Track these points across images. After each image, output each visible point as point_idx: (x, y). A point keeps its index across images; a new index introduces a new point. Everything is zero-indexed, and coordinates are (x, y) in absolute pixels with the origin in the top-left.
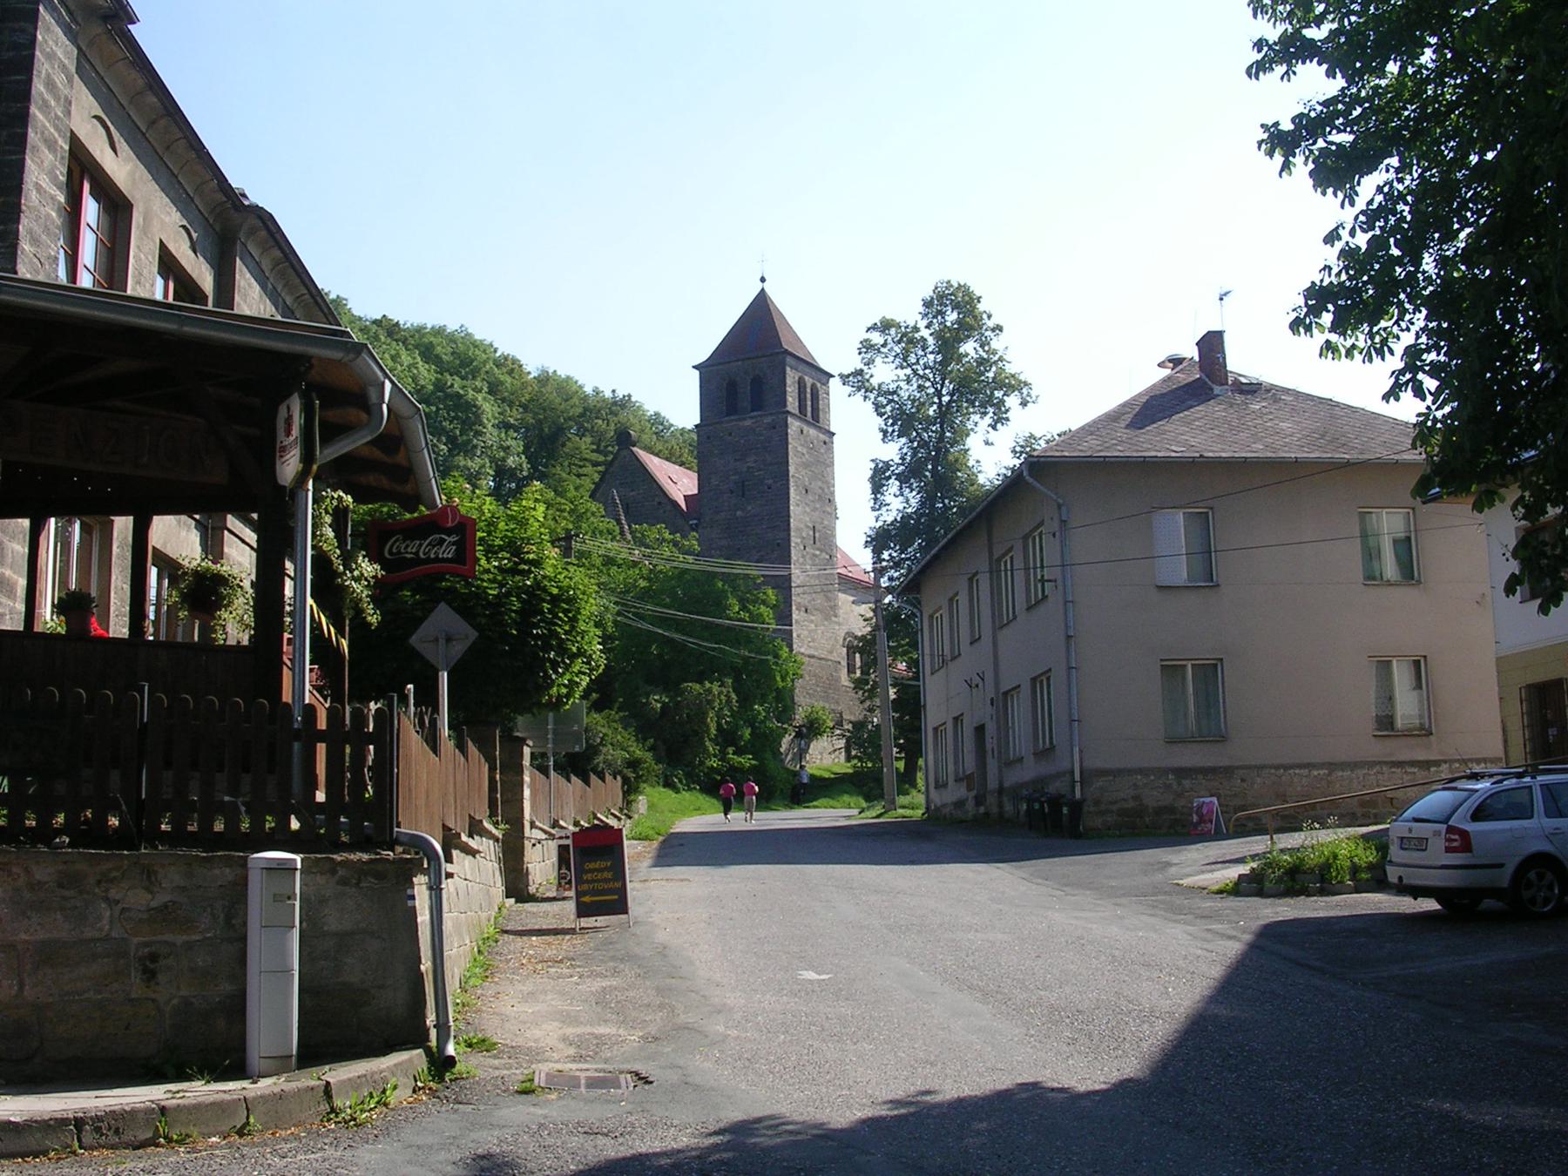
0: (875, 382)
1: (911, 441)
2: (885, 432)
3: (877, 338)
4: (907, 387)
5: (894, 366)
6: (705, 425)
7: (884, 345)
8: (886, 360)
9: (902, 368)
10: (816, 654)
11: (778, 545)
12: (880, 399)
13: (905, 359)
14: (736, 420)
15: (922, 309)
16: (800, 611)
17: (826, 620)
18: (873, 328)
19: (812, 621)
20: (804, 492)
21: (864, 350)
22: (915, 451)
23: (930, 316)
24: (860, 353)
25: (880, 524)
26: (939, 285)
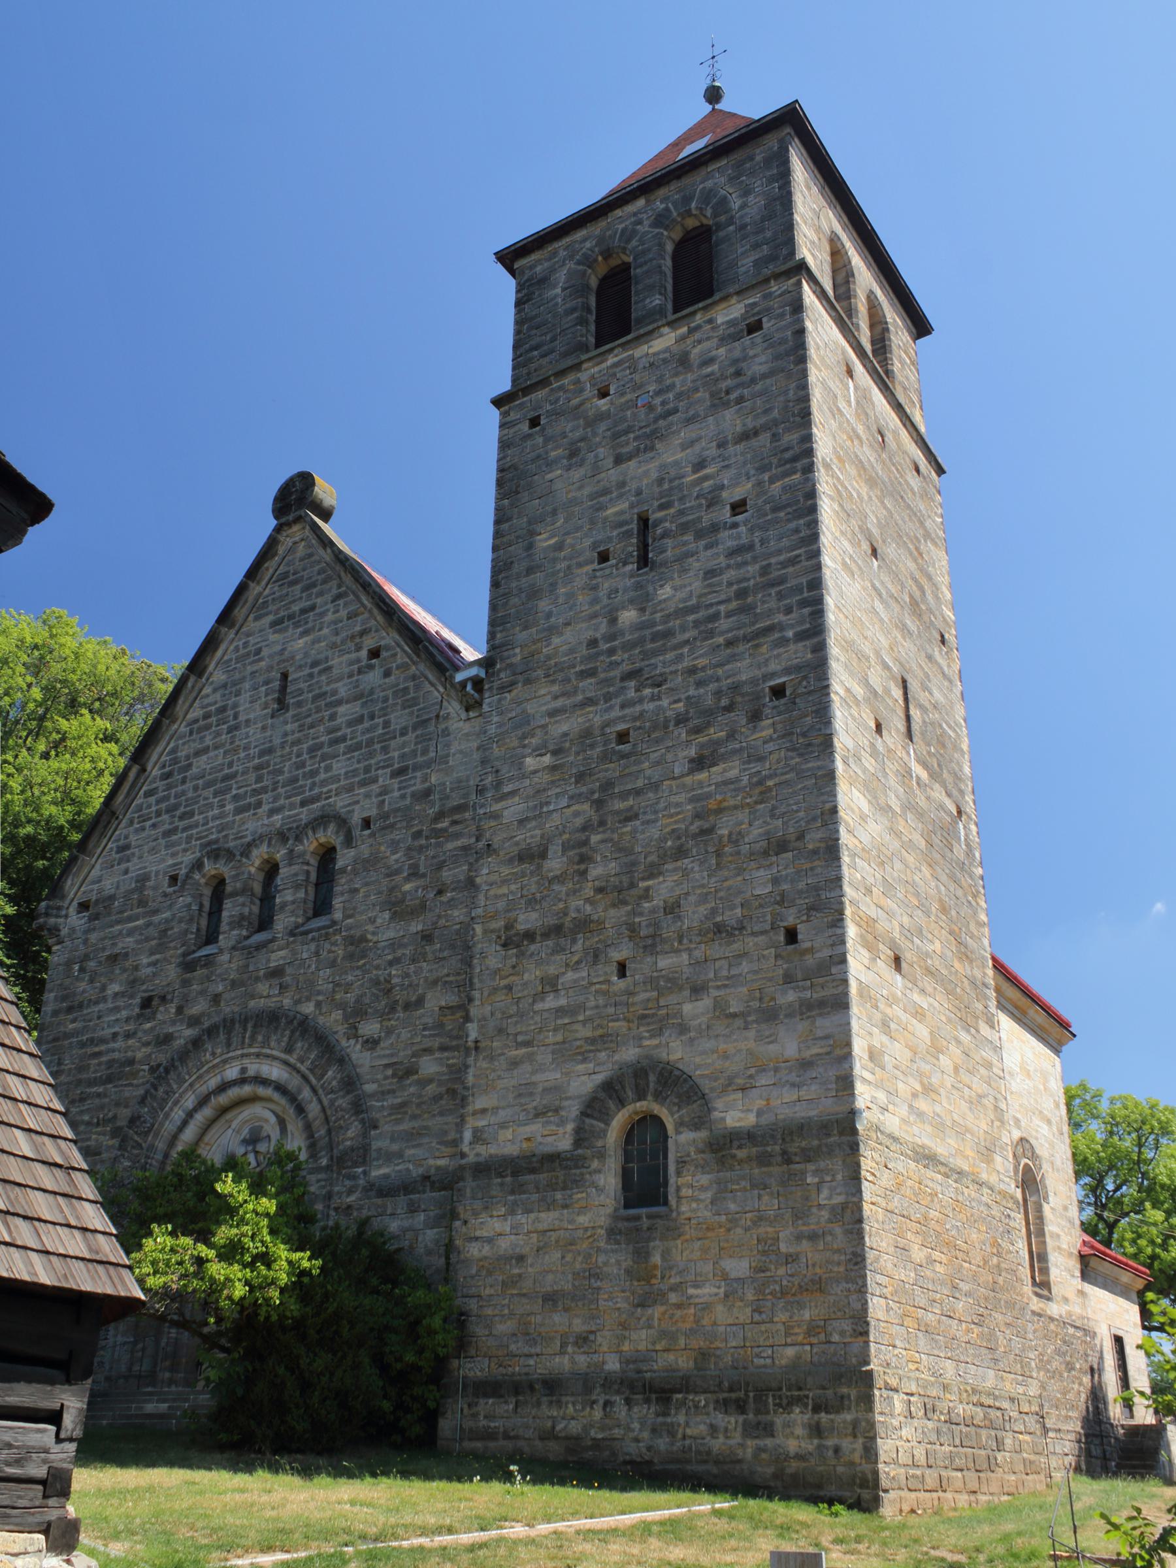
10: (941, 1150)
11: (778, 692)
17: (967, 1027)
19: (919, 1014)
20: (866, 547)
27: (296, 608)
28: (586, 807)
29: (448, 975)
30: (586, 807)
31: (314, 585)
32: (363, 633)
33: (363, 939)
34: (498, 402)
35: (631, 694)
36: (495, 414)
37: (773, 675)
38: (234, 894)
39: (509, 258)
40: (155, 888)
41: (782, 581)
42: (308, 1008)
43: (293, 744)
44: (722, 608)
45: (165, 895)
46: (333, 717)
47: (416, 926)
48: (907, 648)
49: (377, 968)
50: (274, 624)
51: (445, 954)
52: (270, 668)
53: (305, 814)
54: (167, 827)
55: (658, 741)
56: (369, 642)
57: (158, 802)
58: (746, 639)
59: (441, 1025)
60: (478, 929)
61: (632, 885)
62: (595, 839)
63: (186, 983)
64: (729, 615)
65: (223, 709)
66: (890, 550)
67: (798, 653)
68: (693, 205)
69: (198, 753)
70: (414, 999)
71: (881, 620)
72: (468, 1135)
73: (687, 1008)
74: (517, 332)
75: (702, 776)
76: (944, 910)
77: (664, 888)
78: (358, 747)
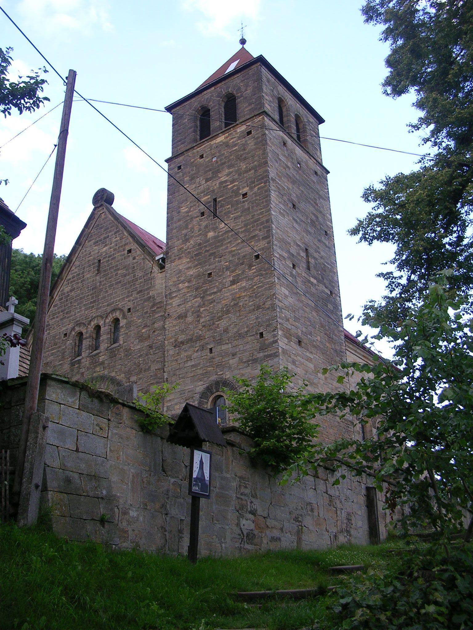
11: (257, 257)
16: (289, 340)
19: (309, 360)
20: (290, 205)
27: (102, 237)
28: (199, 299)
29: (158, 359)
30: (199, 299)
31: (108, 229)
32: (125, 245)
33: (130, 349)
34: (167, 161)
35: (212, 260)
38: (86, 338)
39: (169, 109)
40: (59, 339)
41: (258, 220)
42: (113, 374)
43: (103, 285)
44: (240, 230)
45: (63, 340)
46: (116, 275)
47: (147, 343)
48: (308, 238)
49: (135, 358)
50: (94, 243)
51: (157, 352)
52: (94, 259)
53: (109, 309)
54: (62, 317)
55: (220, 276)
56: (128, 248)
57: (58, 309)
59: (156, 375)
60: (166, 342)
61: (214, 324)
62: (202, 309)
63: (72, 370)
64: (242, 232)
65: (79, 275)
66: (302, 205)
67: (263, 244)
68: (230, 90)
69: (71, 291)
70: (147, 367)
71: (297, 230)
72: (165, 409)
73: (231, 362)
74: (173, 136)
75: (234, 286)
76: (322, 326)
77: (223, 324)
78: (125, 284)
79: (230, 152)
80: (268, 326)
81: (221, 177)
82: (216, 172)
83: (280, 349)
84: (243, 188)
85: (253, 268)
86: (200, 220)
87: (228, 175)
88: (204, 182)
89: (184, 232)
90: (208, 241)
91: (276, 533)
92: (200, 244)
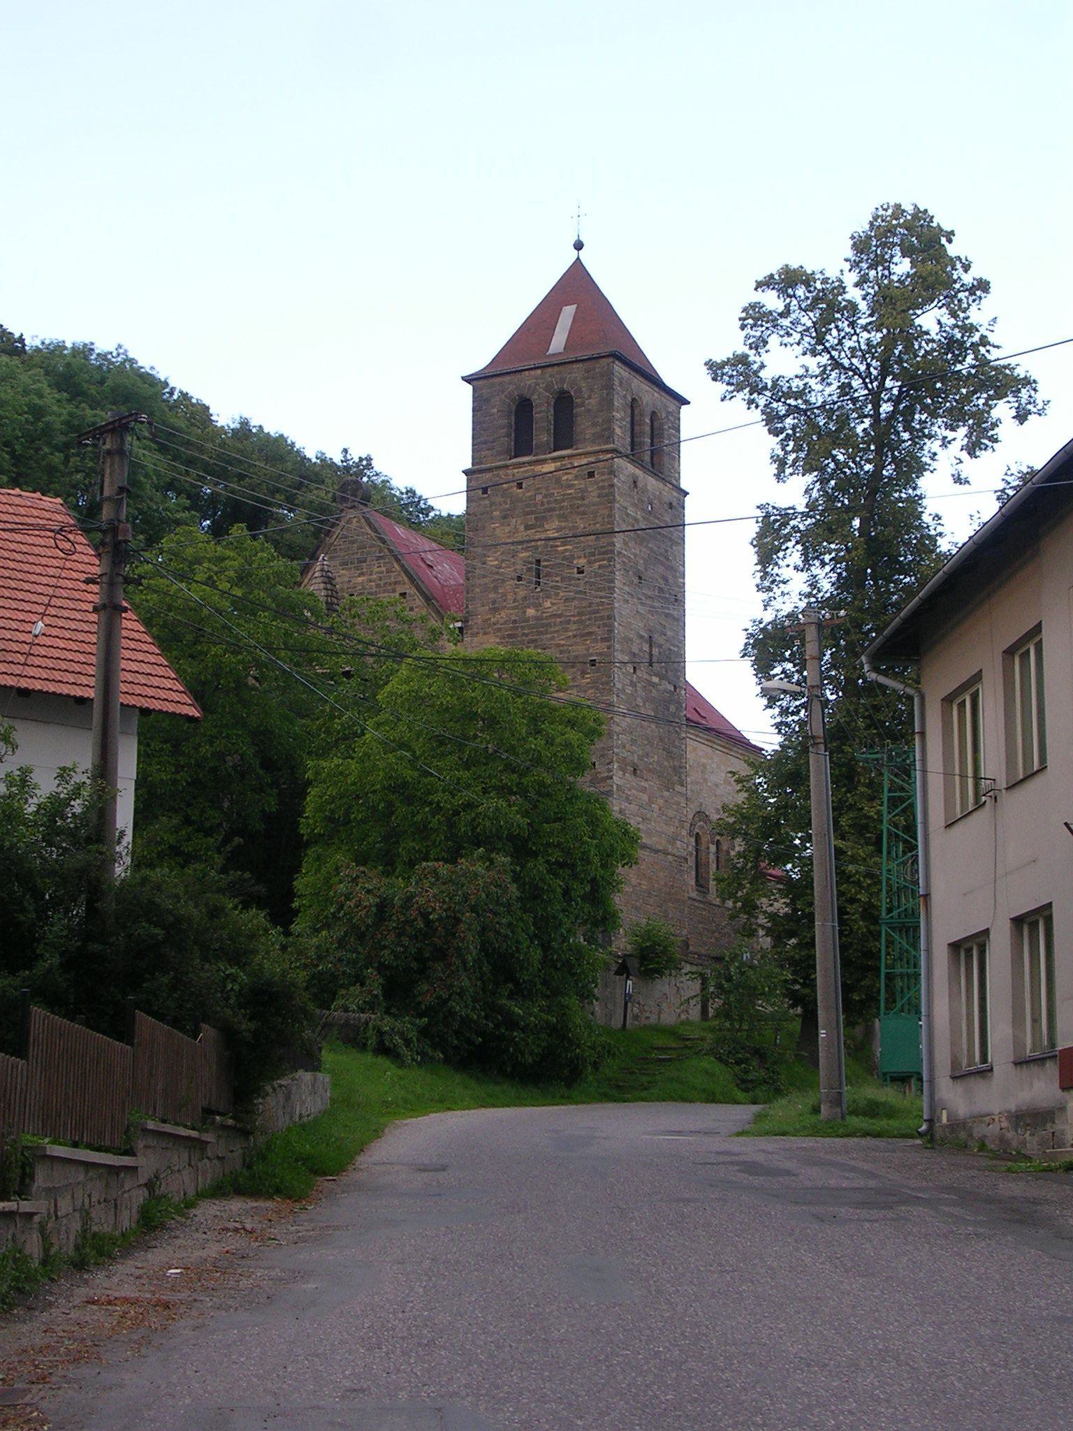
0: (767, 376)
1: (823, 481)
2: (781, 463)
3: (772, 301)
4: (819, 387)
5: (799, 349)
6: (481, 471)
7: (786, 313)
8: (786, 340)
9: (814, 353)
11: (593, 663)
12: (775, 405)
13: (820, 340)
14: (530, 463)
15: (850, 254)
16: (624, 771)
18: (765, 284)
19: (644, 790)
20: (636, 580)
21: (750, 321)
22: (830, 498)
23: (864, 265)
24: (743, 327)
25: (768, 617)
26: (881, 212)
32: (396, 583)
34: (466, 472)
36: (464, 477)
37: (591, 655)
39: (468, 379)
41: (597, 612)
44: (572, 619)
56: (400, 589)
58: (582, 636)
64: (575, 623)
67: (601, 647)
68: (565, 386)
76: (661, 740)
79: (564, 495)
80: (602, 756)
81: (549, 530)
82: (541, 520)
83: (615, 787)
84: (579, 557)
85: (587, 676)
86: (517, 586)
87: (559, 530)
88: (522, 528)
89: (491, 596)
90: (527, 620)
91: (648, 1015)
92: (515, 622)
